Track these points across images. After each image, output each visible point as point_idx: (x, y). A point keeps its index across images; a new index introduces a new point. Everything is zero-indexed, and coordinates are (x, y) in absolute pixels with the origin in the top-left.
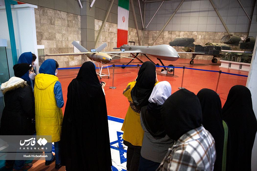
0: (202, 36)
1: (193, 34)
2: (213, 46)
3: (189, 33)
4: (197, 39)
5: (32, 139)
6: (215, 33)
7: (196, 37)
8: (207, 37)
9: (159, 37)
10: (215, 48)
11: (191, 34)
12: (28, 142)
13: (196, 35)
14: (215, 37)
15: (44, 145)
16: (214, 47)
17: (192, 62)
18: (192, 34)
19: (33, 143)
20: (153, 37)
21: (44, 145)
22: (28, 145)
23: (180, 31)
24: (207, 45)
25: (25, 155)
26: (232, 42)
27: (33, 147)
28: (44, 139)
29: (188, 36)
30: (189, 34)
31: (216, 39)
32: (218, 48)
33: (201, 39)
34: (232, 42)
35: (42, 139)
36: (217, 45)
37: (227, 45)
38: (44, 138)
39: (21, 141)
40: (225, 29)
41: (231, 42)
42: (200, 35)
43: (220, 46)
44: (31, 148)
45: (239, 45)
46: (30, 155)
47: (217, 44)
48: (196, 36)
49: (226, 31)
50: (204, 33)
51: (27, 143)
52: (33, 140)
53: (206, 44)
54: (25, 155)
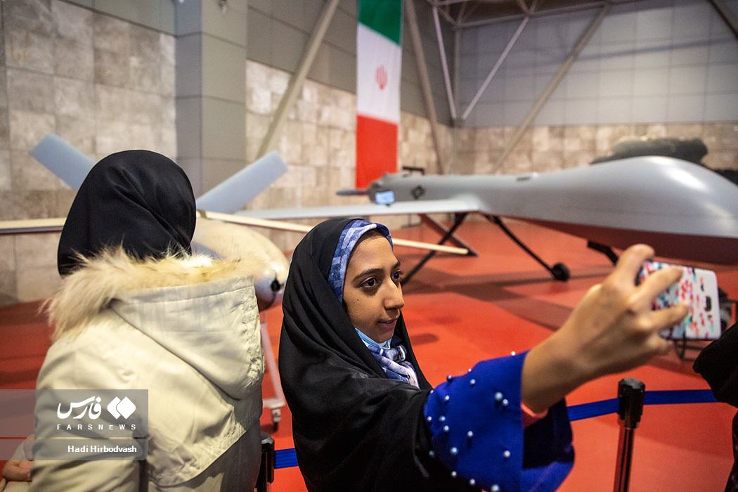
5: (92, 399)
9: (516, 149)
12: (82, 409)
15: (126, 417)
19: (95, 410)
20: (491, 151)
21: (126, 417)
22: (80, 417)
25: (71, 447)
27: (95, 423)
28: (126, 400)
35: (121, 399)
38: (126, 398)
39: (60, 404)
44: (90, 427)
46: (86, 447)
51: (75, 412)
52: (95, 402)
54: (71, 447)
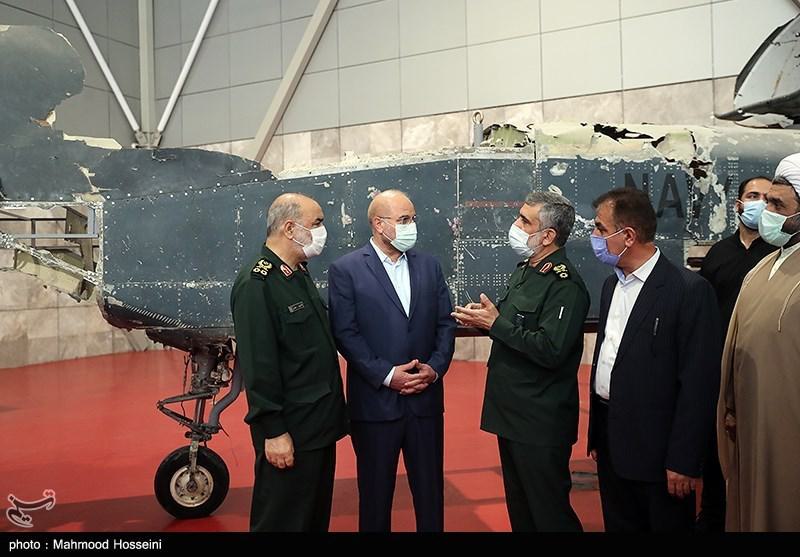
2: (525, 166)
17: (181, 478)
36: (607, 150)
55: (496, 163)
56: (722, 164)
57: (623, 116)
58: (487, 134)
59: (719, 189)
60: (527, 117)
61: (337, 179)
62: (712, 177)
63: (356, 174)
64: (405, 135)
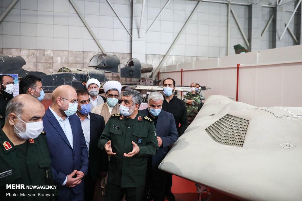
0: (62, 58)
1: (46, 53)
2: (71, 74)
3: (38, 52)
4: (54, 64)
6: (84, 53)
7: (53, 60)
8: (71, 60)
10: (75, 78)
11: (43, 54)
13: (52, 55)
14: (84, 59)
16: (73, 75)
18: (44, 54)
23: (20, 49)
24: (61, 72)
26: (106, 65)
29: (37, 57)
30: (38, 54)
31: (86, 62)
32: (81, 76)
33: (61, 63)
34: (106, 65)
36: (79, 72)
37: (98, 72)
40: (99, 47)
41: (105, 65)
42: (59, 56)
43: (86, 73)
45: (119, 70)
47: (80, 70)
48: (52, 57)
49: (100, 51)
50: (66, 53)
53: (60, 70)
55: (68, 74)
56: (90, 74)
57: (68, 55)
58: (64, 68)
59: (89, 77)
60: (50, 53)
61: (53, 75)
62: (89, 75)
63: (55, 75)
64: (21, 52)
